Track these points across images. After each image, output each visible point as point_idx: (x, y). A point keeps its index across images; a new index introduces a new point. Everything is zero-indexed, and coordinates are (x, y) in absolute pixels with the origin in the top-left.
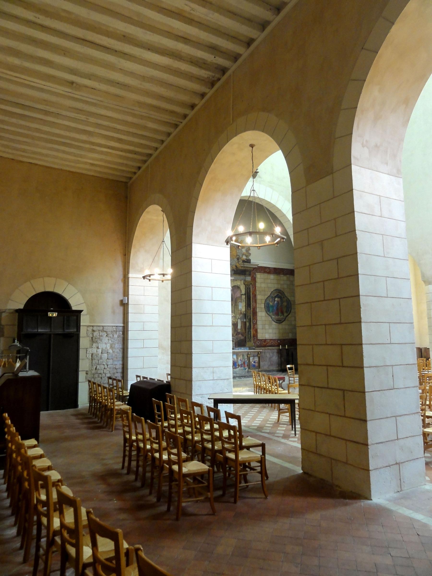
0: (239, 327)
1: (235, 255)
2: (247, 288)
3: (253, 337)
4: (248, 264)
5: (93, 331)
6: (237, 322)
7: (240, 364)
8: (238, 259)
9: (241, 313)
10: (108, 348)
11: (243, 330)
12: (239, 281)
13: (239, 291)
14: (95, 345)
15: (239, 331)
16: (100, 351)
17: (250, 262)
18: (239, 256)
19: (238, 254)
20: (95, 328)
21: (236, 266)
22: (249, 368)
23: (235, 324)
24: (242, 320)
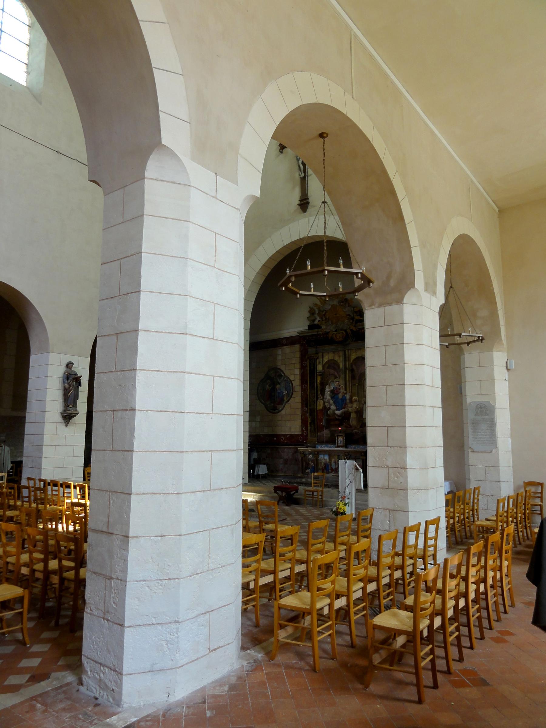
21: (352, 330)
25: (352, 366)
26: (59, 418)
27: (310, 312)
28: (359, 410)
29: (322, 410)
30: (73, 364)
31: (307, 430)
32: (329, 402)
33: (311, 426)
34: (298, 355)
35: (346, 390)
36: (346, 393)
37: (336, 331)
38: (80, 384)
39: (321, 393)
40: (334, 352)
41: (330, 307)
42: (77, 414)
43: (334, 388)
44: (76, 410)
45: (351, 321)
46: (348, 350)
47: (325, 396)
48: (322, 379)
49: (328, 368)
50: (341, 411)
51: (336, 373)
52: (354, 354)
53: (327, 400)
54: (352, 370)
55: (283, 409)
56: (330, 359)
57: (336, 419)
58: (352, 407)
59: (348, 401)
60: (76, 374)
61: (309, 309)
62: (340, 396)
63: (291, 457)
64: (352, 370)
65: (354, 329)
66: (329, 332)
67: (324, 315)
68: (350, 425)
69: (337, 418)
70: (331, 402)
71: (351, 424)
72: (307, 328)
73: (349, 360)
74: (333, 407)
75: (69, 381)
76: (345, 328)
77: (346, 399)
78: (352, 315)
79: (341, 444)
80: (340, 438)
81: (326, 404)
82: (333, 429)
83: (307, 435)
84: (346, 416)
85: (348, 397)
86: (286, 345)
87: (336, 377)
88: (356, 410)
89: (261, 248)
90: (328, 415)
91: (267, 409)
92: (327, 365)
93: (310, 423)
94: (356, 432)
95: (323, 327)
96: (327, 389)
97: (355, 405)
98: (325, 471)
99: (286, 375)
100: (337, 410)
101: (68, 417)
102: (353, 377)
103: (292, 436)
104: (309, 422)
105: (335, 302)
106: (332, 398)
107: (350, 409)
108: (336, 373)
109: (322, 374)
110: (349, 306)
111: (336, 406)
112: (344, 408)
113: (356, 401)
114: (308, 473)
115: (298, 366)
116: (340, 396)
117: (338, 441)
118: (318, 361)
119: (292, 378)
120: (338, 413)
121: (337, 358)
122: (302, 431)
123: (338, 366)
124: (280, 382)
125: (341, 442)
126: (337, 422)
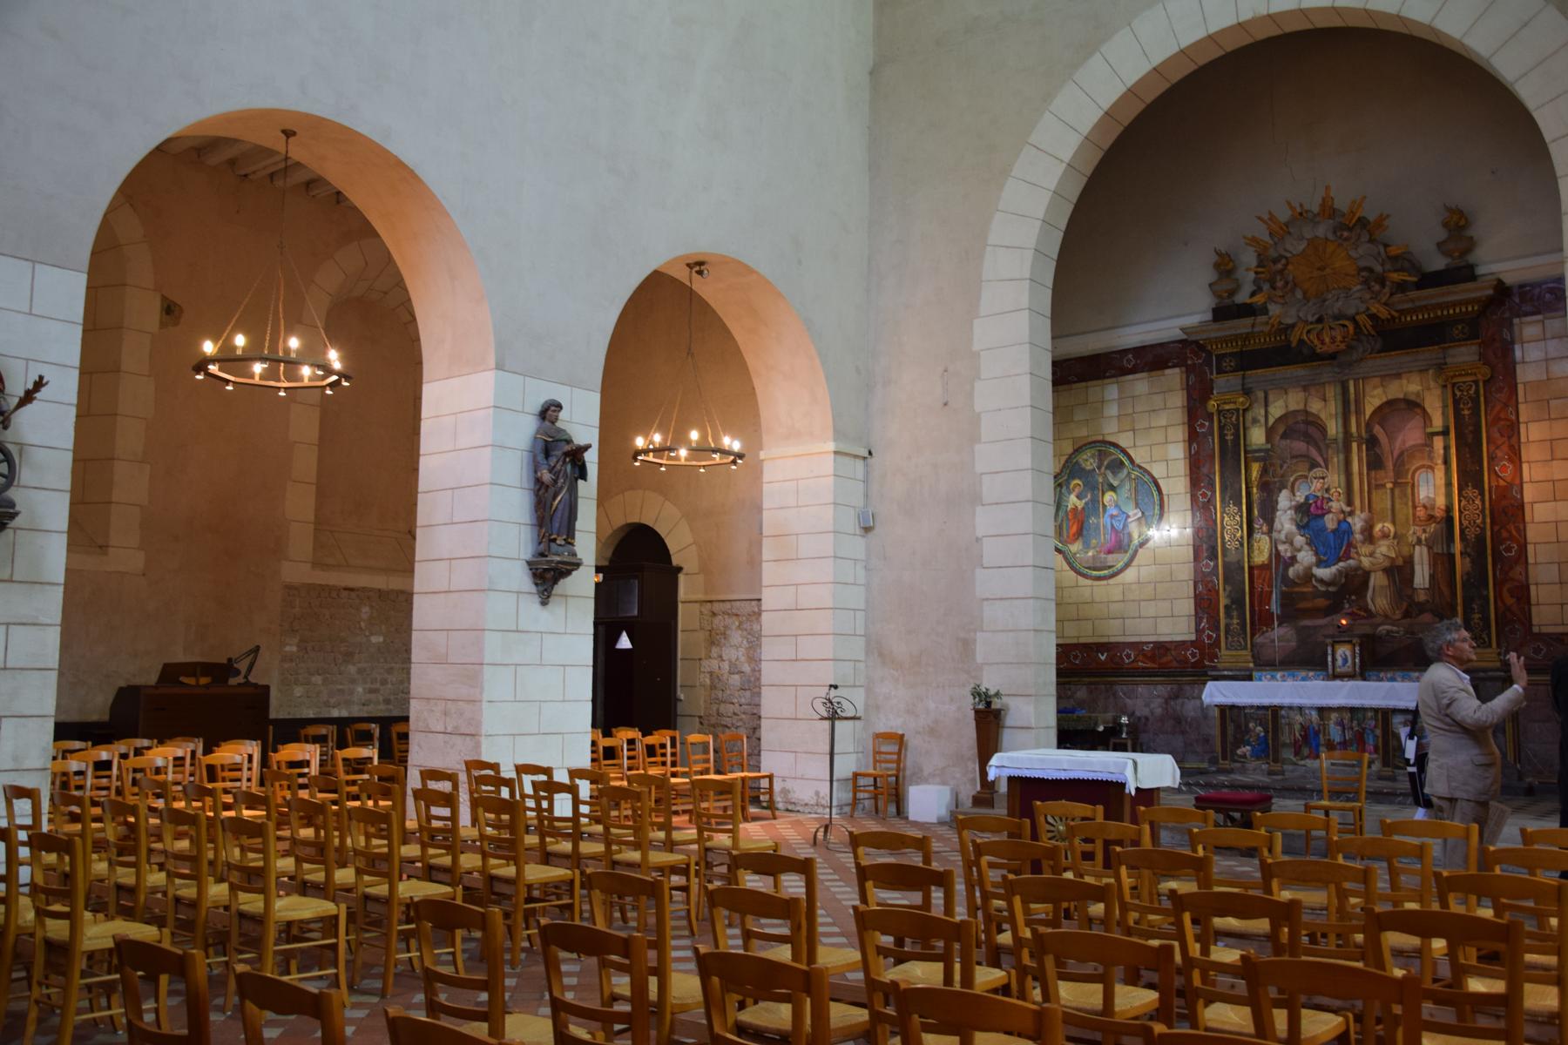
2: (1456, 402)
4: (1470, 285)
5: (714, 614)
6: (1411, 557)
7: (1337, 739)
8: (1366, 282)
9: (1431, 518)
10: (743, 659)
12: (1416, 378)
13: (1417, 422)
14: (715, 651)
15: (1422, 597)
16: (726, 666)
17: (1473, 277)
18: (1370, 270)
19: (1362, 263)
20: (717, 607)
21: (1373, 317)
22: (1385, 763)
23: (1399, 568)
24: (1438, 549)
25: (1368, 425)
26: (522, 579)
27: (1217, 266)
28: (1400, 562)
29: (1263, 567)
30: (559, 406)
31: (1217, 629)
32: (1289, 541)
33: (1228, 615)
34: (1178, 400)
35: (1350, 503)
36: (1351, 513)
37: (1320, 320)
38: (583, 474)
39: (1263, 515)
40: (1305, 388)
41: (1302, 246)
42: (577, 565)
43: (1307, 498)
44: (575, 555)
45: (1377, 287)
46: (1356, 380)
47: (1277, 525)
48: (1264, 471)
50: (1334, 569)
51: (1314, 453)
52: (1379, 391)
53: (1282, 536)
54: (1372, 442)
55: (1127, 565)
56: (1293, 407)
57: (1317, 594)
59: (1358, 537)
60: (569, 441)
61: (1215, 258)
62: (1330, 522)
63: (1159, 711)
64: (1372, 442)
65: (1384, 313)
66: (1293, 326)
67: (1281, 272)
68: (1367, 610)
69: (1322, 588)
70: (1299, 540)
72: (1209, 316)
73: (1359, 412)
74: (1306, 557)
75: (553, 461)
76: (1352, 311)
77: (1350, 532)
78: (1378, 269)
79: (1348, 668)
80: (1343, 651)
81: (1281, 548)
82: (1307, 622)
83: (1217, 643)
84: (1353, 585)
85: (1357, 523)
86: (1133, 371)
87: (1314, 465)
88: (1387, 564)
89: (1096, 61)
90: (1285, 579)
91: (1073, 568)
92: (1281, 430)
93: (1226, 607)
95: (1274, 309)
96: (1284, 500)
97: (1384, 549)
98: (1306, 751)
99: (1138, 461)
100: (1320, 563)
101: (547, 575)
102: (1375, 463)
103: (1162, 648)
104: (1223, 601)
105: (1322, 230)
107: (1366, 562)
110: (1371, 241)
111: (1316, 554)
112: (1347, 557)
113: (1385, 536)
114: (1244, 756)
115: (1179, 433)
116: (1330, 522)
117: (1334, 660)
118: (1249, 416)
119: (1157, 471)
120: (1324, 573)
121: (1315, 406)
122: (1198, 631)
123: (1323, 429)
124: (1115, 483)
125: (1345, 660)
126: (1321, 602)
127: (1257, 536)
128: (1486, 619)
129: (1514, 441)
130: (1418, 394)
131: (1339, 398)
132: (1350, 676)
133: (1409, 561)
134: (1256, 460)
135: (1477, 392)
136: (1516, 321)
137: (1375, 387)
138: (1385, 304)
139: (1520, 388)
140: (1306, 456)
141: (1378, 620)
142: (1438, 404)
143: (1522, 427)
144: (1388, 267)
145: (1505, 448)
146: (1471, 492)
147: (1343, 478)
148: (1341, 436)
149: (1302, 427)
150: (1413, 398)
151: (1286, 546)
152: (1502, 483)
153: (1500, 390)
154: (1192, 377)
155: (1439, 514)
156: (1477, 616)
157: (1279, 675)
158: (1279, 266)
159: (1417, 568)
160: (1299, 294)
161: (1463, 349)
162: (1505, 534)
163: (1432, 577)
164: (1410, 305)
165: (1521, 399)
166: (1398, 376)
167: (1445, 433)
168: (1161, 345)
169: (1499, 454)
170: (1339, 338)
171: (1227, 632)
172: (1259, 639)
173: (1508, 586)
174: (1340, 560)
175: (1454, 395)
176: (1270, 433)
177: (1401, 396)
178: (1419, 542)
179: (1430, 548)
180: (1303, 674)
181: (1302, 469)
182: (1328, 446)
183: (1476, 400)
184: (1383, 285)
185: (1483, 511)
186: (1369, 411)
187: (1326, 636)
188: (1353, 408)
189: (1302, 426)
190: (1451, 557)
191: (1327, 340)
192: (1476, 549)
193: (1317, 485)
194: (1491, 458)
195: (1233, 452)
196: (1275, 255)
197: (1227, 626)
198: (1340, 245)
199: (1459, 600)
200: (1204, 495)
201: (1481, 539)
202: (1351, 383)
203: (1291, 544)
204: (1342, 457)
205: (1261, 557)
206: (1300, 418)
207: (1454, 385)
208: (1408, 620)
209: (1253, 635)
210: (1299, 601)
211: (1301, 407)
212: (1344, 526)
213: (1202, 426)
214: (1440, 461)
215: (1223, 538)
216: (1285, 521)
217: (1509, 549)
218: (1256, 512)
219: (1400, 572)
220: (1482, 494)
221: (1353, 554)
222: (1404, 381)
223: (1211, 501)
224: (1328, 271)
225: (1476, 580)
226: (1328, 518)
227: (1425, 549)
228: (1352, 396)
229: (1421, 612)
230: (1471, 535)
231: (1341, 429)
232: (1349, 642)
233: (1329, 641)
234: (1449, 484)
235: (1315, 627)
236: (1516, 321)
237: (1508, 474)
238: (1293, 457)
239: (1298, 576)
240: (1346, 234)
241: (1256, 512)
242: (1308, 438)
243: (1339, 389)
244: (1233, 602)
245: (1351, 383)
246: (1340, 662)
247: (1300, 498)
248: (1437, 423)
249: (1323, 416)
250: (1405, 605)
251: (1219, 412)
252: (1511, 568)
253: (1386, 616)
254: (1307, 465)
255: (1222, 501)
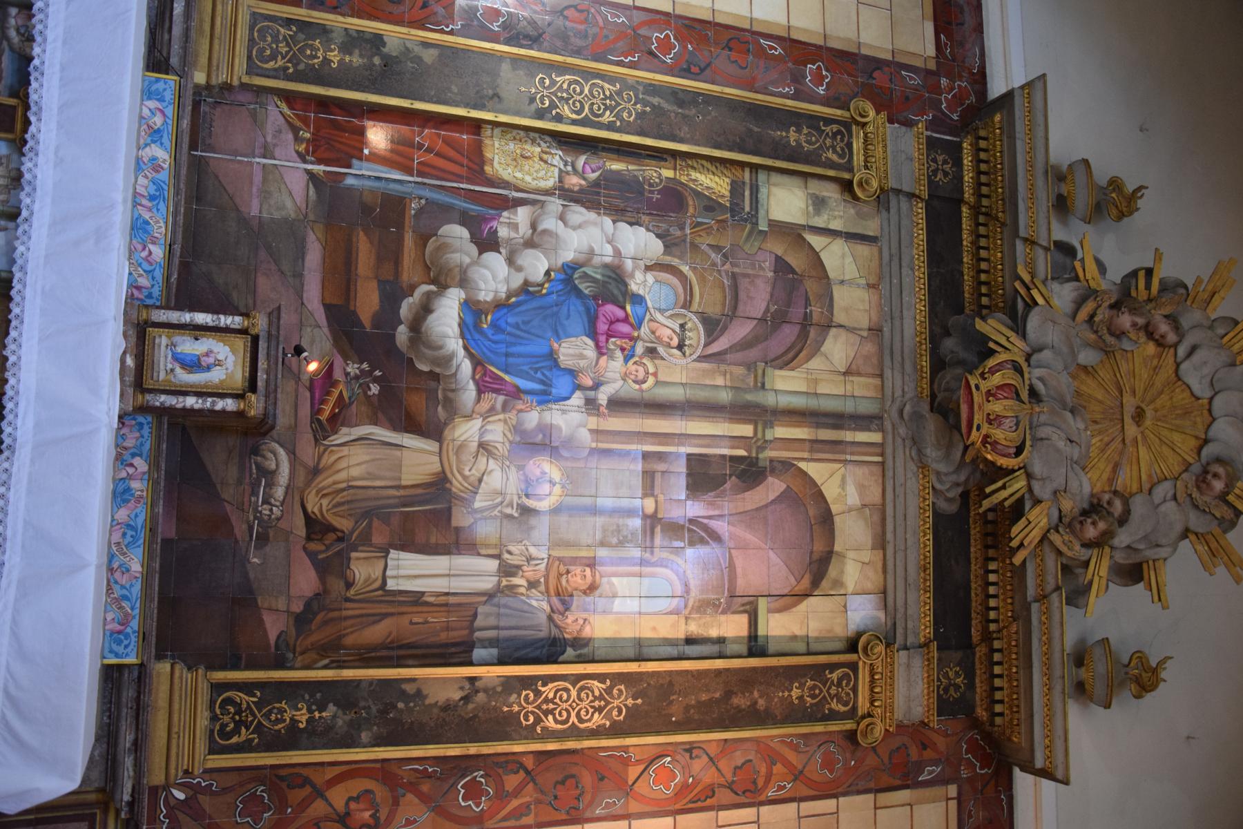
0: (412, 571)
1: (1125, 479)
2: (818, 671)
3: (278, 779)
8: (1094, 509)
9: (564, 599)
11: (376, 633)
12: (874, 579)
15: (363, 569)
18: (1123, 521)
19: (1139, 506)
21: (1017, 511)
23: (443, 517)
25: (785, 467)
29: (476, 164)
33: (353, 41)
34: (873, 37)
35: (619, 405)
36: (591, 404)
37: (1033, 393)
40: (875, 330)
43: (638, 299)
45: (1091, 532)
46: (880, 448)
47: (579, 214)
48: (710, 205)
49: (781, 266)
50: (455, 345)
51: (740, 331)
52: (853, 498)
53: (549, 223)
56: (841, 296)
57: (393, 294)
58: (482, 446)
64: (749, 471)
68: (336, 421)
69: (406, 308)
70: (537, 265)
71: (345, 434)
73: (815, 445)
74: (494, 277)
77: (545, 397)
79: (164, 366)
80: (225, 362)
81: (522, 215)
82: (314, 256)
87: (713, 327)
88: (457, 484)
90: (438, 213)
92: (796, 261)
94: (270, 476)
95: (1063, 295)
96: (637, 242)
100: (473, 310)
102: (703, 476)
104: (395, 34)
106: (567, 276)
107: (466, 431)
108: (740, 331)
109: (740, 212)
110: (1186, 533)
111: (499, 305)
112: (486, 384)
116: (575, 350)
118: (831, 192)
121: (837, 349)
123: (787, 360)
125: (193, 365)
126: (367, 302)
127: (557, 157)
128: (292, 738)
129: (725, 796)
130: (838, 583)
131: (849, 407)
132: (138, 377)
133: (454, 542)
134: (736, 188)
135: (833, 716)
136: (953, 790)
137: (861, 488)
138: (1044, 538)
139: (829, 805)
140: (733, 312)
141: (307, 451)
142: (814, 628)
143: (748, 813)
144: (1120, 557)
145: (710, 776)
146: (623, 700)
147: (677, 394)
148: (770, 400)
149: (797, 312)
150: (832, 572)
151: (524, 230)
152: (633, 772)
153: (828, 764)
154: (916, 81)
155: (572, 623)
156: (302, 717)
157: (162, 154)
158: (1164, 328)
159: (439, 563)
160: (1087, 357)
161: (920, 688)
162: (512, 781)
163: (416, 599)
164: (1031, 592)
165: (808, 807)
166: (881, 543)
167: (755, 645)
168: (979, 28)
169: (698, 765)
170: (998, 434)
171: (303, 26)
172: (276, 114)
173: (381, 792)
174: (477, 363)
175: (833, 667)
176: (792, 233)
177: (837, 548)
178: (508, 570)
179: (490, 596)
180: (160, 227)
181: (709, 300)
182: (750, 366)
183: (817, 714)
184: (1087, 545)
185: (575, 733)
186: (814, 470)
187: (275, 316)
188: (826, 434)
189: (797, 312)
190: (459, 653)
191: (997, 407)
192: (477, 719)
193: (667, 328)
194: (690, 749)
195: (763, 139)
196: (1185, 322)
197: (323, 31)
198: (1187, 467)
199: (348, 674)
200: (665, 46)
201: (505, 727)
202: (875, 437)
203: (530, 244)
204: (725, 397)
205: (504, 160)
206: (816, 310)
207: (854, 667)
208: (299, 527)
209: (289, 98)
210: (378, 243)
211: (839, 317)
212: (561, 385)
213: (819, 79)
214: (694, 629)
215: (563, 69)
216: (589, 236)
217: (474, 791)
218: (617, 166)
219: (429, 517)
220: (616, 730)
221: (490, 399)
222: (866, 556)
223: (650, 58)
224: (1131, 430)
225: (397, 717)
226: (586, 347)
227: (487, 584)
228: (848, 436)
229: (323, 569)
230: (522, 705)
231: (784, 401)
232: (252, 386)
233: (260, 323)
234: (640, 651)
235: (299, 275)
236: (953, 790)
237: (653, 787)
238: (734, 277)
239: (443, 248)
240: (1218, 485)
241: (617, 166)
242: (773, 321)
243: (866, 408)
244: (388, 62)
245: (875, 437)
246: (189, 346)
247: (640, 282)
248: (776, 626)
249: (816, 363)
250: (344, 524)
251: (847, 125)
252: (424, 798)
253: (316, 471)
254: (714, 310)
255: (652, 89)
